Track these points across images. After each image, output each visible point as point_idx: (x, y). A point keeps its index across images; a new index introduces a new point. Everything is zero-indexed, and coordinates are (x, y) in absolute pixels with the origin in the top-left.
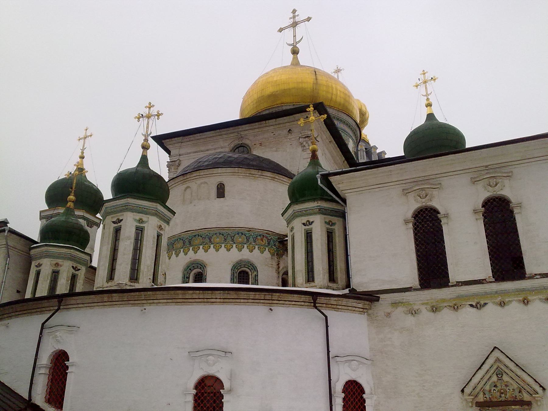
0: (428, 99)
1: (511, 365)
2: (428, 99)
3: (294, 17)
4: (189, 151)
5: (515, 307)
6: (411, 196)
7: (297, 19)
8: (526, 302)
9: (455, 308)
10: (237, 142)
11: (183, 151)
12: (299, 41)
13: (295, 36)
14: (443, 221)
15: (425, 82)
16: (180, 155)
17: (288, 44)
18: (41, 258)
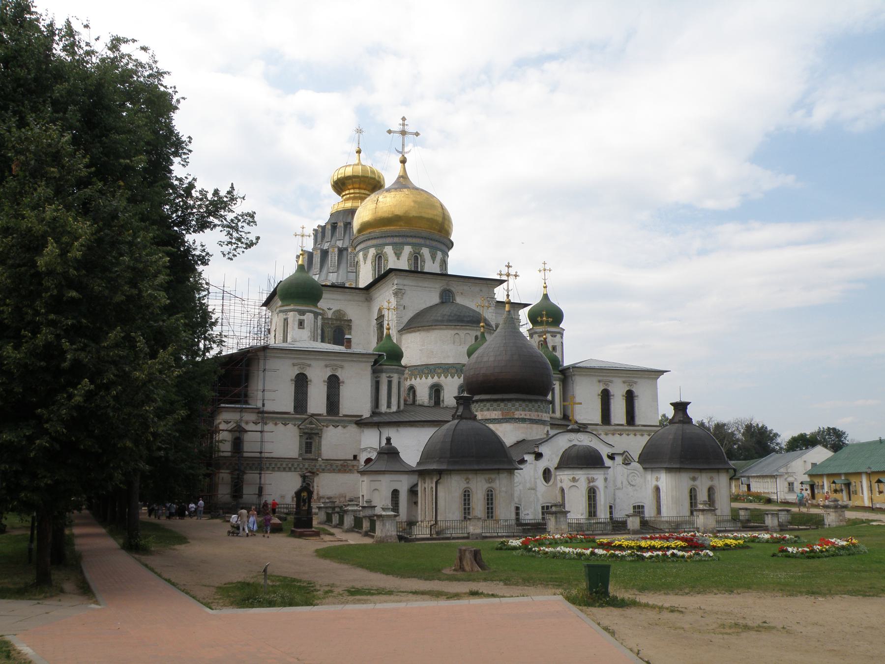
0: (545, 283)
1: (629, 456)
2: (545, 283)
3: (404, 125)
4: (411, 284)
5: (632, 436)
6: (601, 383)
7: (407, 129)
8: (635, 435)
9: (613, 434)
10: (445, 287)
11: (406, 282)
12: (407, 153)
13: (403, 145)
14: (612, 397)
15: (545, 270)
16: (404, 285)
17: (396, 150)
18: (392, 372)
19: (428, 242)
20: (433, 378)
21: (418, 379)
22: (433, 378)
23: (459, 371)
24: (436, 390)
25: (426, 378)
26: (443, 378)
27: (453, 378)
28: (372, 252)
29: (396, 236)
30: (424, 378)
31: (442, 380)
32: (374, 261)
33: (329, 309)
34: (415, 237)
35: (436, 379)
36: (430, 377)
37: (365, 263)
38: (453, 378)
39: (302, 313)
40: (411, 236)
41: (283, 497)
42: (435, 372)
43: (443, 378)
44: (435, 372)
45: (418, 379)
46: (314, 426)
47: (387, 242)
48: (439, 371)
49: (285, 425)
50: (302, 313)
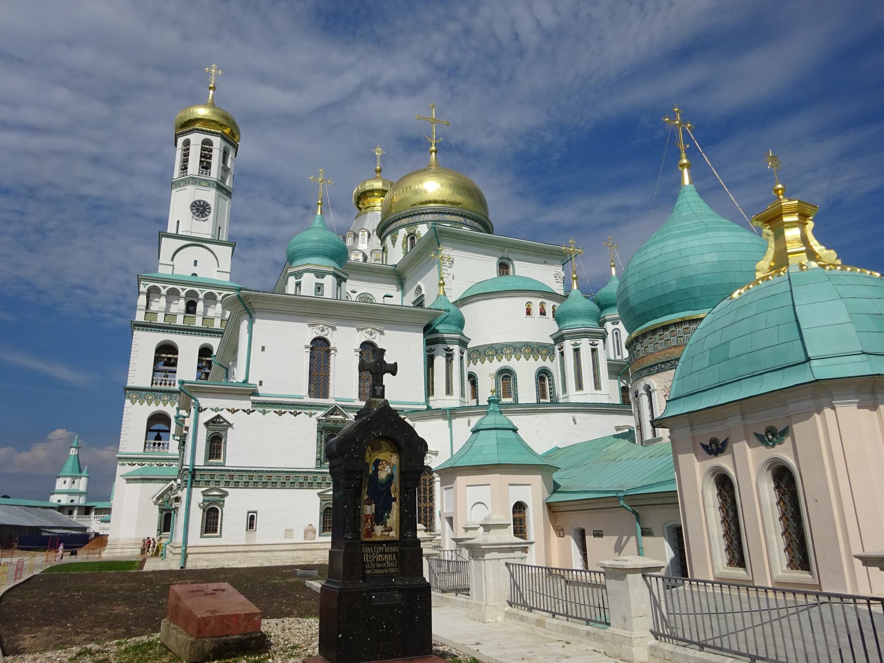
19: (468, 221)
20: (500, 361)
21: (479, 363)
22: (500, 361)
23: (535, 351)
24: (506, 375)
25: (491, 362)
26: (513, 358)
27: (527, 360)
28: (403, 232)
29: (431, 213)
30: (487, 361)
31: (512, 363)
32: (405, 242)
33: (353, 292)
34: (453, 214)
35: (504, 363)
36: (495, 360)
37: (394, 247)
38: (527, 360)
39: (320, 274)
40: (449, 213)
41: (289, 532)
42: (502, 353)
43: (513, 358)
44: (502, 353)
45: (479, 363)
46: (340, 417)
47: (421, 220)
48: (508, 351)
49: (295, 416)
50: (320, 274)
